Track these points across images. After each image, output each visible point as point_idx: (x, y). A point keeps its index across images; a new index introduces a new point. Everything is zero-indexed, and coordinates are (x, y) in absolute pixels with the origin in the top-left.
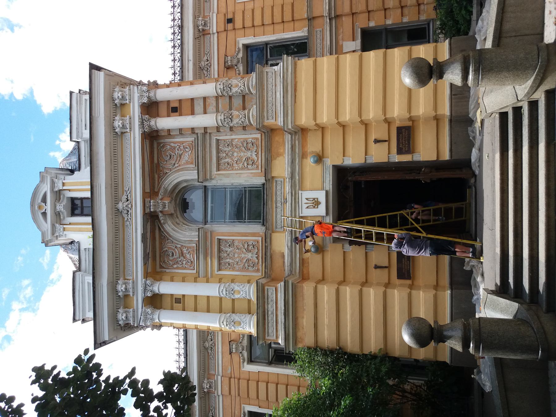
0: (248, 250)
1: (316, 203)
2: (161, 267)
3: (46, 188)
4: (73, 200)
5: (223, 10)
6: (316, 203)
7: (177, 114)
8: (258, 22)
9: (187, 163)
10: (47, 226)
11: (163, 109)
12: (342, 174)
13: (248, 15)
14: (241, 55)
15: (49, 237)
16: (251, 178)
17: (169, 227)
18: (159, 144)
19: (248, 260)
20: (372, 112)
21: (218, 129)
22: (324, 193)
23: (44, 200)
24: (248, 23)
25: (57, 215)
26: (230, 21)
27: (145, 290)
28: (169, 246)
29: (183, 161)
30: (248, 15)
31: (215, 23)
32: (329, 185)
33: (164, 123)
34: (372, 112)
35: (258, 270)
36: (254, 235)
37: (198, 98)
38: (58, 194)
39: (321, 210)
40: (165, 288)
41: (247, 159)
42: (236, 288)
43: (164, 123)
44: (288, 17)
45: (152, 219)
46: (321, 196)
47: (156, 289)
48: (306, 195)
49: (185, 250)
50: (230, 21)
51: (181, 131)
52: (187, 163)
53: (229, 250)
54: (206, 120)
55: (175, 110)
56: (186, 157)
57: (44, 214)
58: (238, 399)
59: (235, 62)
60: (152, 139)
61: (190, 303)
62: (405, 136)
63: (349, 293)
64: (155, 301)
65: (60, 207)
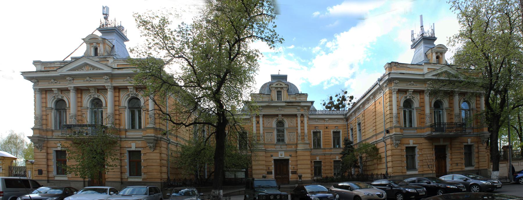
1: (281, 155)
6: (281, 155)
8: (326, 135)
11: (302, 119)
12: (288, 160)
13: (327, 133)
16: (287, 140)
21: (297, 133)
24: (326, 133)
28: (270, 119)
31: (326, 123)
33: (299, 119)
38: (282, 88)
39: (280, 156)
40: (261, 120)
43: (299, 119)
44: (326, 143)
45: (277, 115)
46: (283, 156)
48: (283, 153)
51: (297, 123)
54: (299, 131)
60: (296, 116)
61: (258, 125)
63: (264, 163)
64: (258, 117)
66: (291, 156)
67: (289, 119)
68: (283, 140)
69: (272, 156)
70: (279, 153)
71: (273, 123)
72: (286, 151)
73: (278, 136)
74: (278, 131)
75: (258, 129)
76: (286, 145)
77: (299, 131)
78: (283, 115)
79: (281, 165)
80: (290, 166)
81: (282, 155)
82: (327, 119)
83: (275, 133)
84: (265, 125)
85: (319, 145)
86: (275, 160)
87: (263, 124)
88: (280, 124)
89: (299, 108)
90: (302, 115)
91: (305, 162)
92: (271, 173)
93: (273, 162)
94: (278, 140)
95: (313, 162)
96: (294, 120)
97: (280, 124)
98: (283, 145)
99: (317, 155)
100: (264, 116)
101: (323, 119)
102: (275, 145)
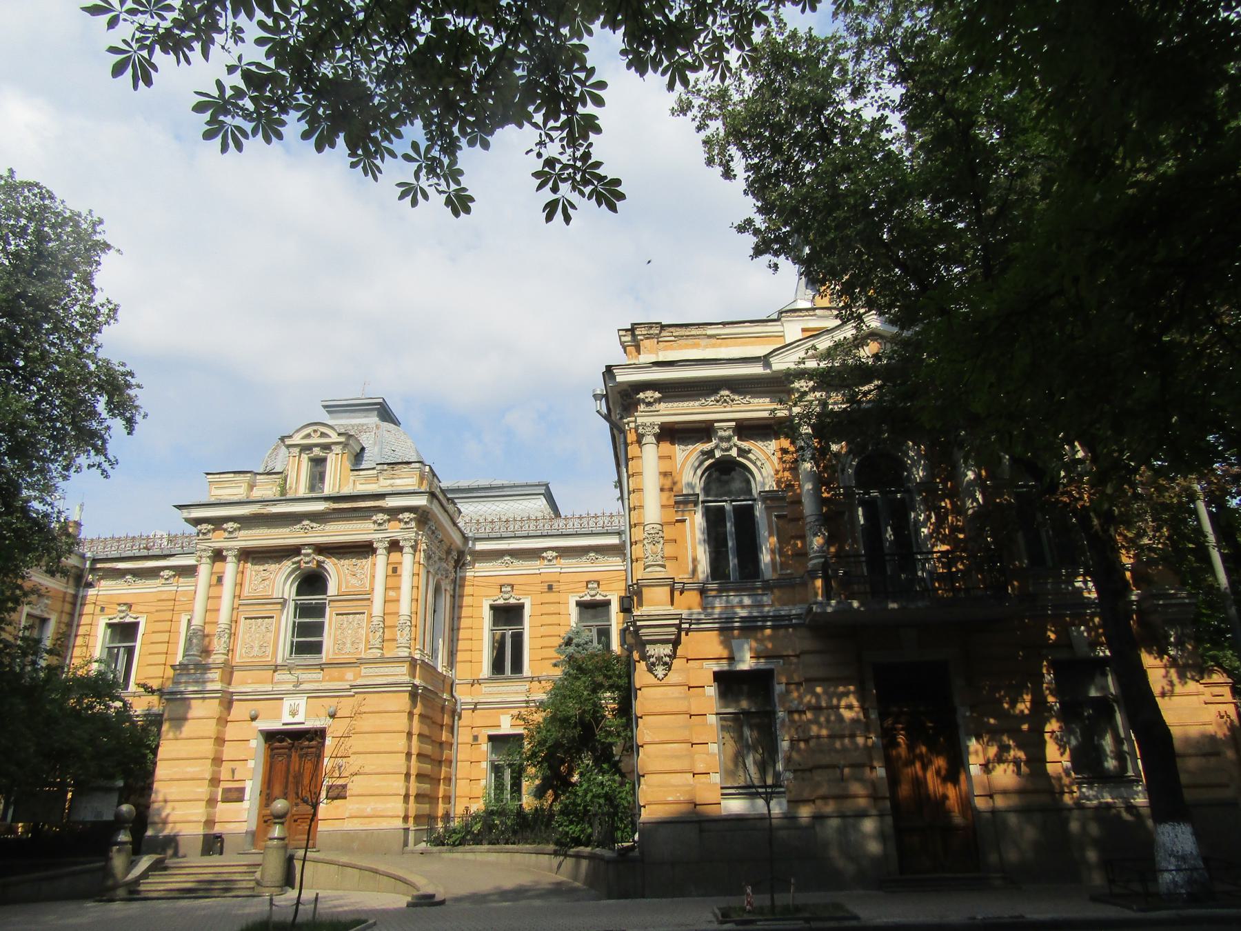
0: (261, 646)
1: (294, 714)
2: (254, 559)
3: (334, 438)
4: (324, 460)
5: (563, 578)
6: (294, 714)
7: (390, 572)
9: (347, 582)
10: (297, 440)
12: (320, 734)
13: (552, 609)
14: (512, 601)
15: (288, 442)
17: (288, 565)
18: (368, 553)
19: (252, 647)
20: (354, 763)
22: (302, 720)
23: (323, 435)
25: (308, 448)
26: (550, 588)
27: (228, 550)
28: (273, 567)
29: (349, 578)
30: (552, 609)
32: (309, 725)
34: (354, 763)
35: (241, 656)
36: (275, 653)
37: (399, 595)
40: (230, 568)
41: (344, 644)
42: (223, 640)
43: (381, 559)
45: (295, 551)
47: (229, 559)
48: (301, 702)
49: (267, 582)
50: (550, 588)
52: (347, 582)
53: (263, 628)
55: (395, 570)
56: (353, 581)
57: (308, 436)
58: (153, 609)
59: (507, 596)
62: (339, 793)
65: (317, 451)
66: (333, 716)
67: (346, 564)
68: (316, 648)
69: (254, 719)
70: (287, 703)
71: (280, 581)
72: (314, 695)
73: (301, 629)
74: (303, 610)
75: (213, 610)
76: (321, 667)
77: (377, 608)
78: (321, 549)
79: (295, 752)
80: (326, 760)
81: (295, 713)
82: (550, 554)
83: (287, 619)
84: (246, 592)
85: (517, 666)
86: (271, 737)
87: (239, 584)
88: (312, 582)
89: (380, 517)
90: (394, 546)
91: (383, 742)
92: (236, 795)
93: (256, 744)
94: (301, 649)
95: (483, 739)
96: (366, 563)
97: (312, 582)
98: (308, 667)
99: (504, 706)
100: (247, 555)
101: (535, 554)
102: (276, 668)
